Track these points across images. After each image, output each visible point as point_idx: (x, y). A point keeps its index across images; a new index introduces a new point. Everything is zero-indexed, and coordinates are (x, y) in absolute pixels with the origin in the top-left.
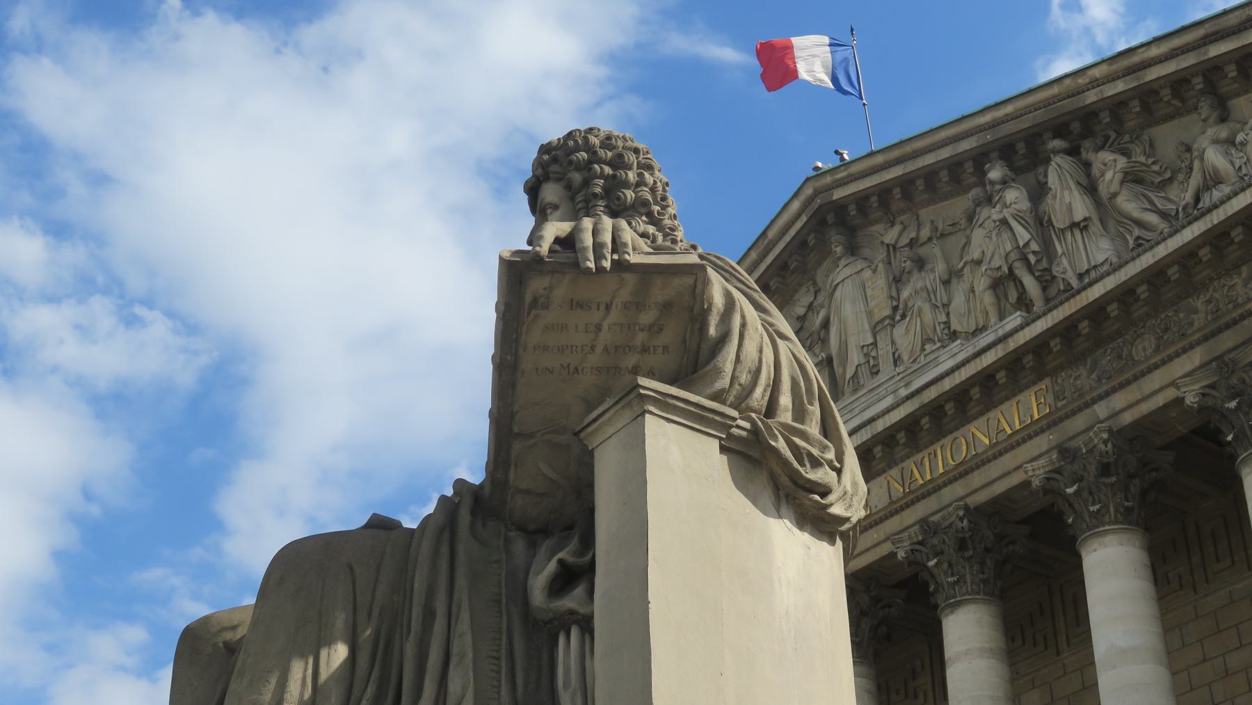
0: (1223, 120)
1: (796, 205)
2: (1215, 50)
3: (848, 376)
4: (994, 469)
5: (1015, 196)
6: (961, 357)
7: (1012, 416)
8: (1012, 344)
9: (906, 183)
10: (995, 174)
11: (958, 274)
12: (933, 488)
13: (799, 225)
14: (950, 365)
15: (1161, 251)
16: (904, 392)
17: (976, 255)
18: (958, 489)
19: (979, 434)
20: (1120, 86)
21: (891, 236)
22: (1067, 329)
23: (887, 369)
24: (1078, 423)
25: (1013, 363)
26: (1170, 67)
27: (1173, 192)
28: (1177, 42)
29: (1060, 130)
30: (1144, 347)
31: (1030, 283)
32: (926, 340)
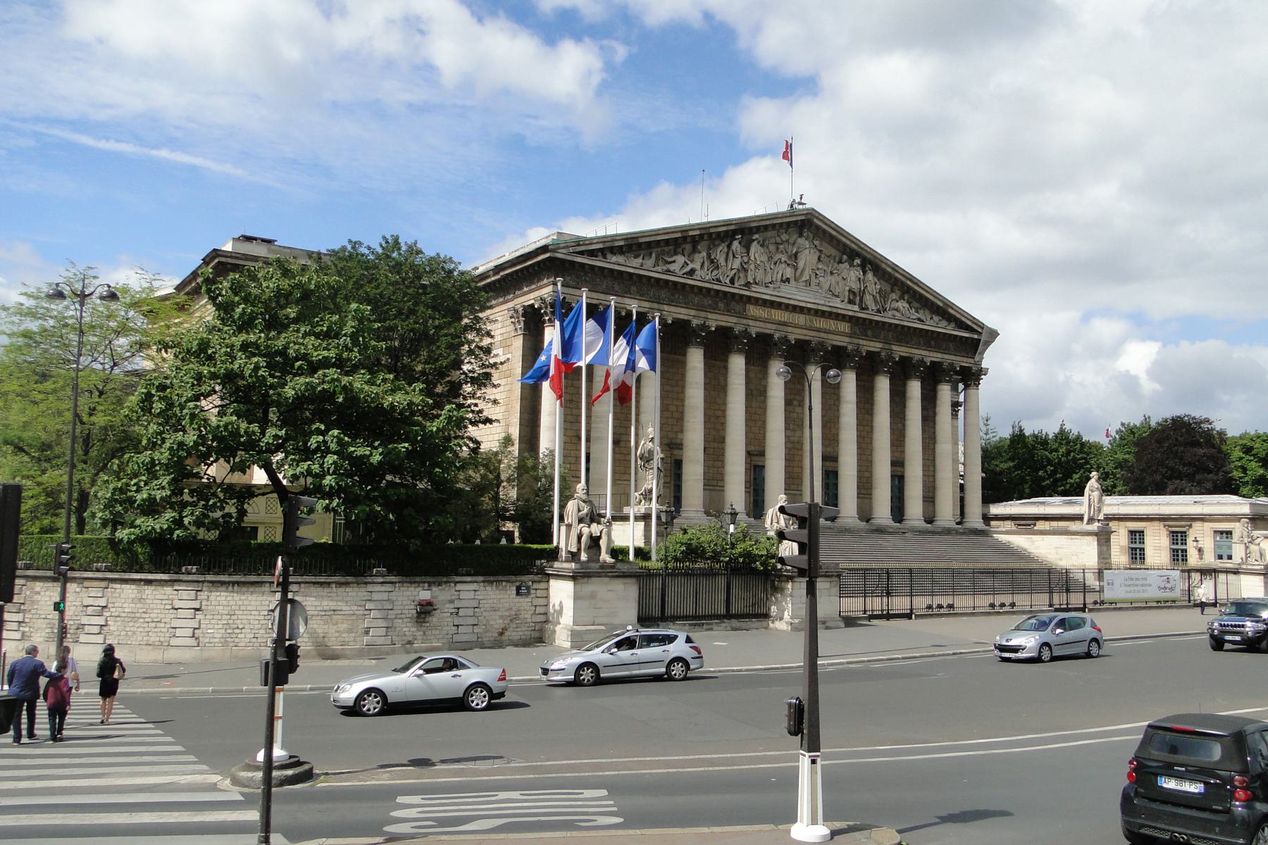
9: (832, 236)
10: (858, 261)
12: (818, 330)
14: (837, 303)
19: (831, 324)
22: (865, 319)
23: (813, 287)
24: (856, 341)
25: (851, 317)
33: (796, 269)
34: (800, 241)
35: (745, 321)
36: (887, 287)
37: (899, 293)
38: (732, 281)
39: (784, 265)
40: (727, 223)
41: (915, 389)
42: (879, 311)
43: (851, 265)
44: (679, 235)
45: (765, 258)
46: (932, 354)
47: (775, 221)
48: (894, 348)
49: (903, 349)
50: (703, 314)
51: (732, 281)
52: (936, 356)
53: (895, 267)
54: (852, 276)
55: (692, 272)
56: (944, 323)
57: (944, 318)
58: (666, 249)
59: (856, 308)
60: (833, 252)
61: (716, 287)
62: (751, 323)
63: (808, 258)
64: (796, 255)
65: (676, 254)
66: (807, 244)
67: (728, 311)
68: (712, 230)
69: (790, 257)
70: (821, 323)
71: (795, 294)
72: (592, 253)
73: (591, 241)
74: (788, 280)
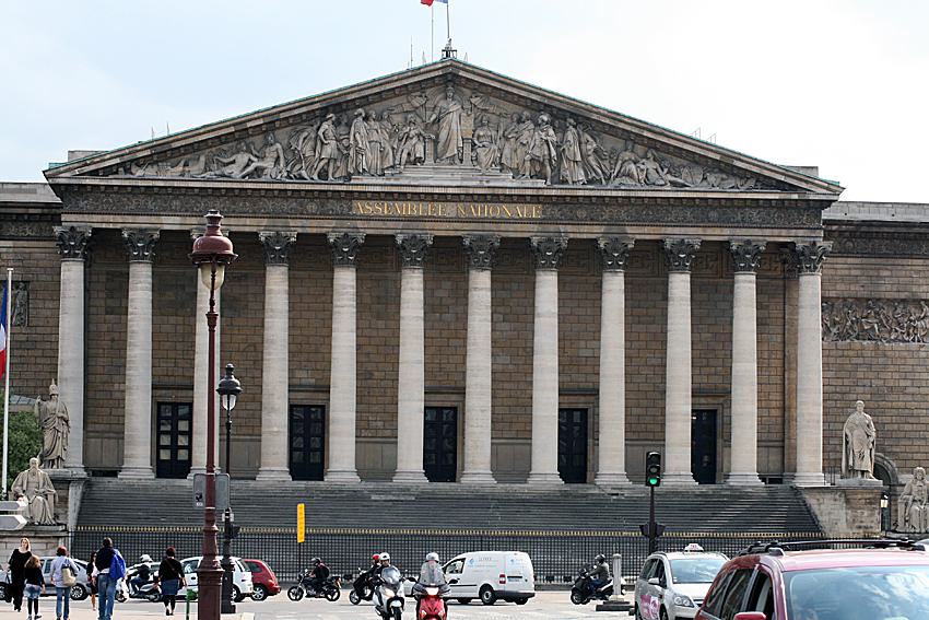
0: (632, 151)
1: (440, 66)
2: (645, 134)
3: (448, 155)
4: (511, 227)
5: (551, 132)
6: (514, 185)
7: (522, 211)
8: (540, 192)
11: (507, 139)
13: (437, 74)
14: (507, 181)
15: (609, 194)
16: (486, 184)
17: (525, 142)
18: (493, 227)
19: (507, 210)
20: (607, 121)
21: (473, 100)
23: (467, 163)
24: (552, 228)
26: (628, 128)
27: (606, 163)
28: (635, 122)
29: (572, 115)
30: (582, 213)
31: (548, 168)
32: (493, 162)
33: (436, 142)
34: (442, 104)
35: (349, 223)
36: (620, 144)
37: (640, 149)
38: (323, 175)
39: (415, 140)
40: (308, 102)
41: (680, 285)
42: (590, 182)
43: (537, 125)
44: (232, 129)
45: (379, 136)
46: (709, 231)
47: (388, 87)
48: (629, 230)
49: (646, 230)
50: (280, 222)
51: (323, 175)
52: (717, 234)
53: (615, 116)
54: (538, 139)
55: (259, 171)
56: (732, 182)
57: (734, 175)
58: (225, 147)
59: (540, 183)
60: (511, 108)
61: (290, 187)
62: (359, 224)
63: (457, 122)
64: (438, 120)
65: (238, 152)
66: (454, 107)
67: (324, 215)
68: (282, 116)
69: (425, 129)
70: (488, 210)
71: (430, 177)
72: (108, 171)
73: (101, 156)
74: (419, 160)
